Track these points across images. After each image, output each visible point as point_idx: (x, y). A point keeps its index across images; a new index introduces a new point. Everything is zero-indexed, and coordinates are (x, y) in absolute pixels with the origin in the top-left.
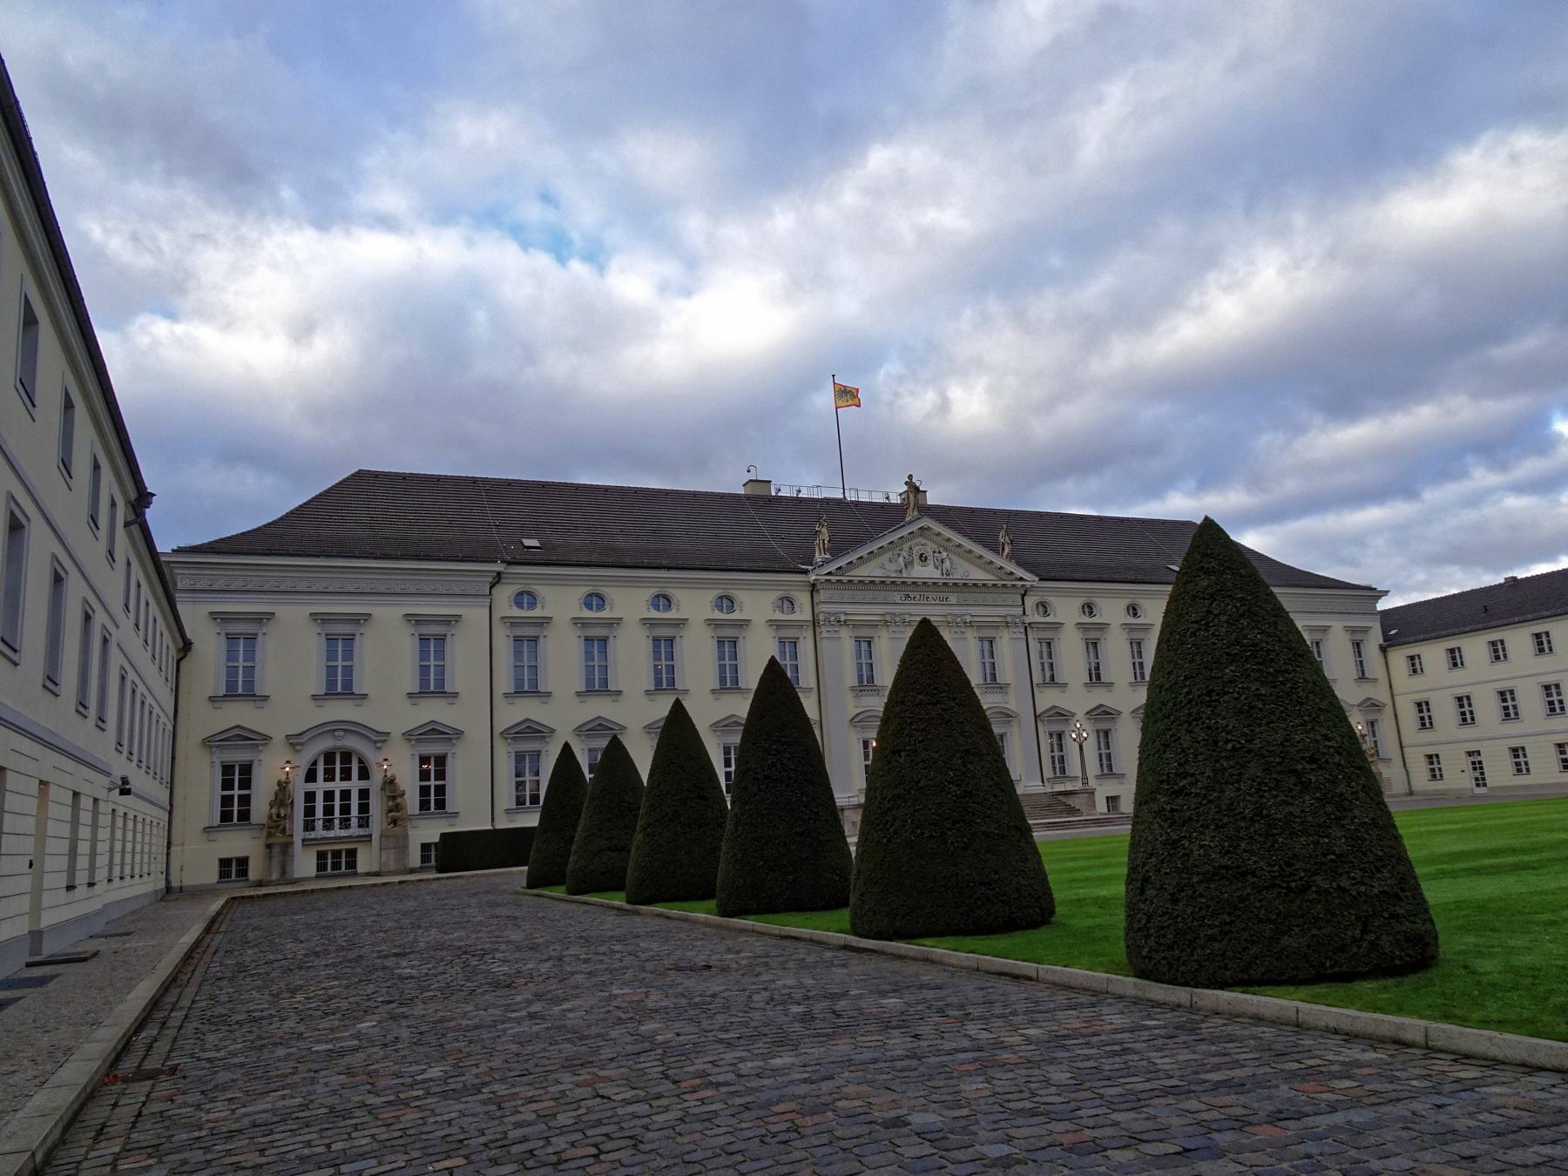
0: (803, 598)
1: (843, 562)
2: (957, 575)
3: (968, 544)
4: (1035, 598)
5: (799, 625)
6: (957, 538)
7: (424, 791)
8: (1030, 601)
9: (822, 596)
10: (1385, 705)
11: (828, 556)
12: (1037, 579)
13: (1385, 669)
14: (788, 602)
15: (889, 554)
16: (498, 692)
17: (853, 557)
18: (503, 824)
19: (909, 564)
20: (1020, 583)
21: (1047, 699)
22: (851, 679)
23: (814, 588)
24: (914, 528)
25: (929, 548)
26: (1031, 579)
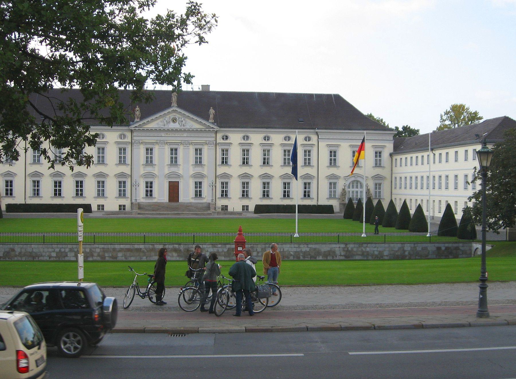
0: (129, 134)
1: (141, 123)
2: (188, 127)
3: (191, 116)
4: (222, 134)
5: (126, 143)
6: (187, 114)
7: (7, 190)
8: (219, 136)
9: (135, 134)
10: (385, 178)
11: (138, 120)
12: (219, 128)
13: (391, 162)
14: (121, 136)
15: (161, 119)
16: (27, 163)
17: (145, 121)
18: (30, 201)
19: (168, 123)
20: (211, 130)
21: (221, 170)
22: (143, 160)
23: (132, 131)
24: (170, 110)
25: (177, 116)
26: (216, 128)
